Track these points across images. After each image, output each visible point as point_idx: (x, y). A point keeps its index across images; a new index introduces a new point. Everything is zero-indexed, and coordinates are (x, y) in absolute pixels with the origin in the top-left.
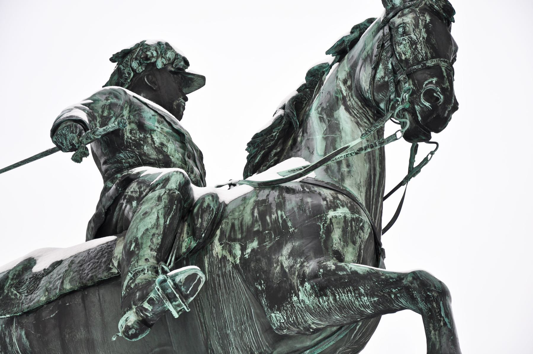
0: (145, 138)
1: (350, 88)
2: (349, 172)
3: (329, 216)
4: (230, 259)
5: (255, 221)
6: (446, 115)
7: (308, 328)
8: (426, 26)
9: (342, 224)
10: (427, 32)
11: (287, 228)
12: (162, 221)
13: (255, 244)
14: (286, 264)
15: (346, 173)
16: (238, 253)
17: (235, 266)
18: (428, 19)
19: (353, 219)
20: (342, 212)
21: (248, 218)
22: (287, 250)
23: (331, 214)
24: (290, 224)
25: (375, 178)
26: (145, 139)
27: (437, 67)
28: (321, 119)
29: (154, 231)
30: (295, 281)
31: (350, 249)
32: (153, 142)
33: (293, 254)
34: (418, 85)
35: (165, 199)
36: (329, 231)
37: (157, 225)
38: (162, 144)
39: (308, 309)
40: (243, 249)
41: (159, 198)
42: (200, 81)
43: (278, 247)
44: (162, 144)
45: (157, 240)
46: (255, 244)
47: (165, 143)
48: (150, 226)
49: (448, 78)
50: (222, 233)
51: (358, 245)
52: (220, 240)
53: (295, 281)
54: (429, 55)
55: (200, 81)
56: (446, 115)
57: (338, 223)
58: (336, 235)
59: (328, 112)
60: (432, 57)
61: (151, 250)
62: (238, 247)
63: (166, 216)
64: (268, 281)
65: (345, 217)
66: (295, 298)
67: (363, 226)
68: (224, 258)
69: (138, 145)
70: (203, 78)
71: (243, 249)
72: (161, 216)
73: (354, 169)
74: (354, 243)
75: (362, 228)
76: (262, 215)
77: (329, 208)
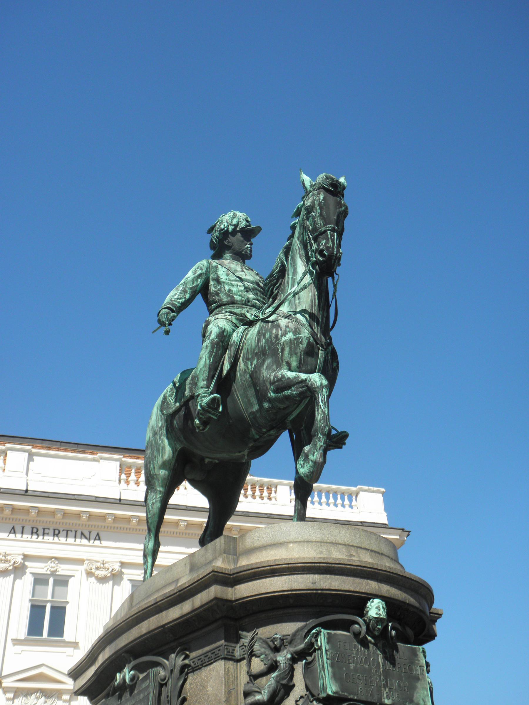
0: (221, 288)
2: (299, 303)
3: (282, 341)
4: (247, 371)
6: (333, 263)
7: (280, 409)
8: (320, 205)
9: (289, 344)
10: (321, 209)
11: (266, 351)
12: (208, 362)
13: (255, 362)
15: (297, 304)
16: (250, 367)
18: (322, 196)
19: (295, 339)
20: (290, 336)
21: (253, 344)
23: (284, 339)
24: (267, 348)
25: (315, 301)
26: (220, 290)
27: (326, 231)
29: (204, 369)
30: (268, 385)
31: (294, 358)
32: (225, 289)
35: (209, 348)
36: (283, 350)
37: (205, 365)
38: (230, 290)
40: (251, 365)
41: (207, 346)
42: (258, 229)
44: (230, 290)
45: (206, 374)
46: (255, 362)
47: (231, 288)
48: (202, 366)
49: (331, 238)
50: (244, 355)
51: (299, 354)
52: (243, 360)
53: (268, 385)
54: (322, 224)
55: (258, 229)
56: (333, 263)
57: (287, 344)
58: (287, 350)
60: (324, 225)
61: (204, 380)
62: (249, 363)
63: (210, 356)
65: (290, 339)
66: (269, 395)
67: (302, 341)
68: (245, 370)
69: (218, 294)
70: (259, 227)
71: (251, 364)
72: (207, 358)
73: (302, 300)
74: (296, 354)
75: (301, 343)
77: (282, 336)
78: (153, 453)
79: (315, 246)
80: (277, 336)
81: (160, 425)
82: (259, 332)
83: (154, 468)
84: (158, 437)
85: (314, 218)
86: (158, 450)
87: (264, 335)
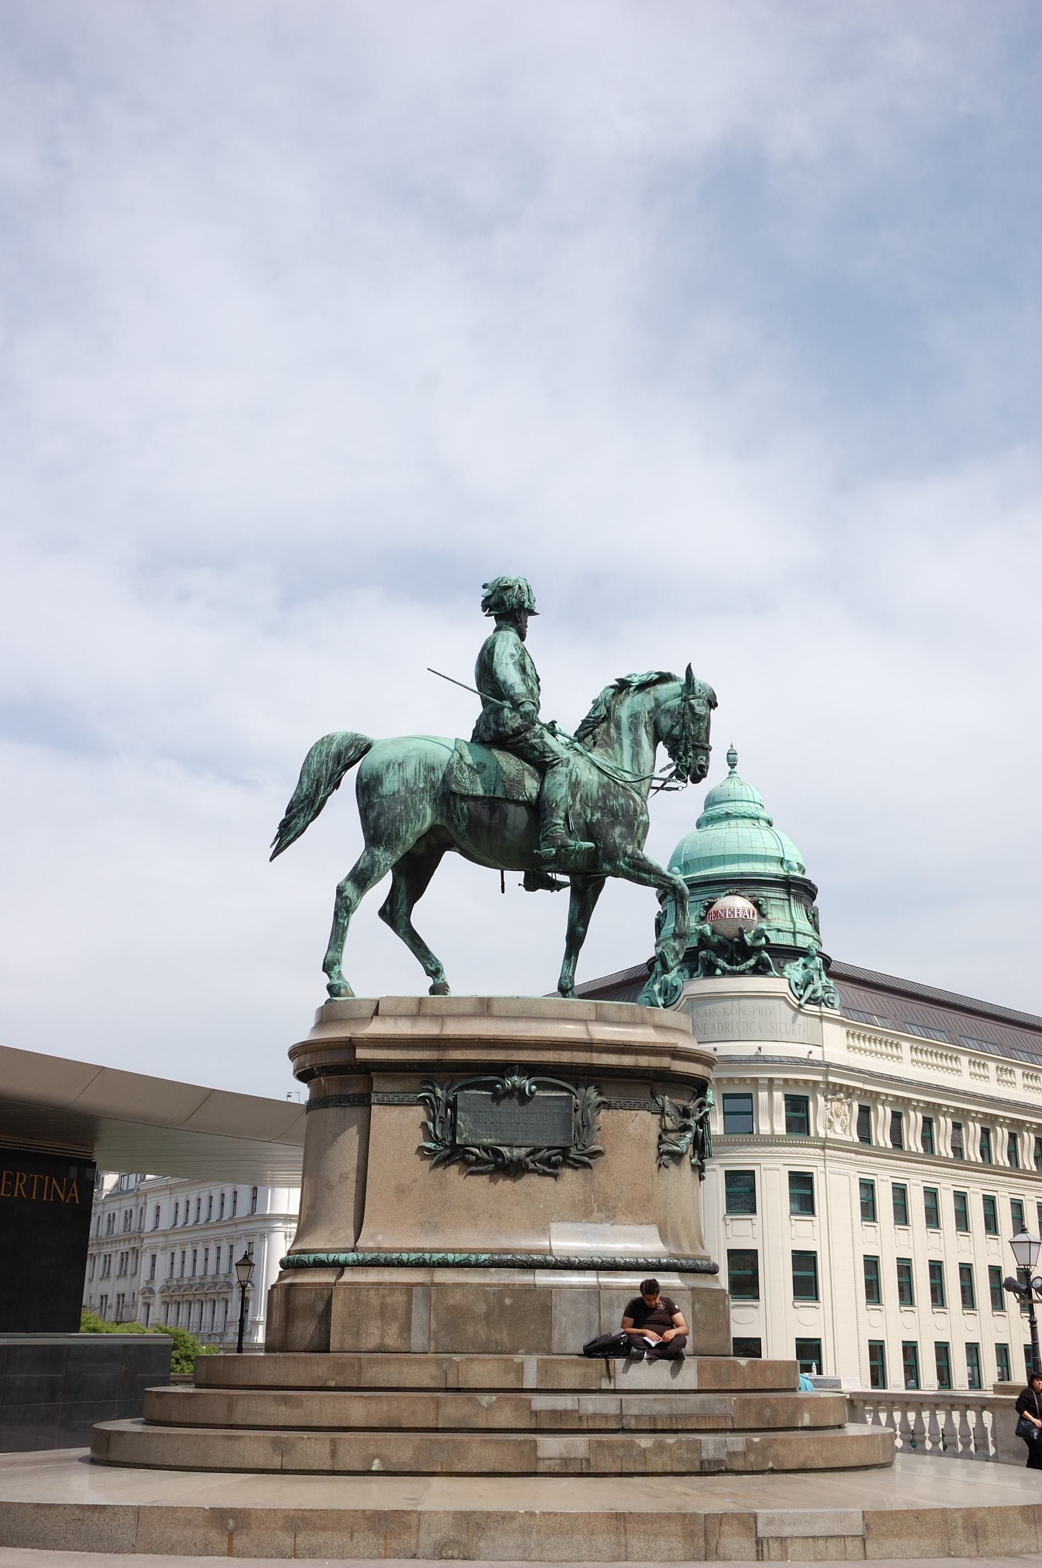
1: (650, 718)
5: (599, 799)
14: (618, 840)
17: (586, 822)
21: (595, 794)
22: (618, 830)
23: (641, 818)
28: (630, 729)
30: (621, 855)
33: (620, 835)
34: (696, 756)
36: (638, 828)
39: (623, 870)
40: (592, 815)
43: (613, 824)
46: (598, 815)
53: (621, 855)
59: (634, 727)
64: (604, 843)
71: (592, 815)
76: (605, 798)
78: (408, 813)
79: (691, 754)
80: (635, 810)
81: (422, 786)
82: (601, 785)
83: (407, 831)
84: (417, 799)
85: (700, 728)
86: (419, 816)
87: (616, 798)
